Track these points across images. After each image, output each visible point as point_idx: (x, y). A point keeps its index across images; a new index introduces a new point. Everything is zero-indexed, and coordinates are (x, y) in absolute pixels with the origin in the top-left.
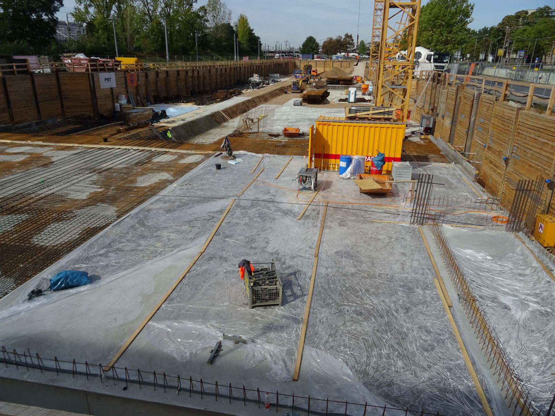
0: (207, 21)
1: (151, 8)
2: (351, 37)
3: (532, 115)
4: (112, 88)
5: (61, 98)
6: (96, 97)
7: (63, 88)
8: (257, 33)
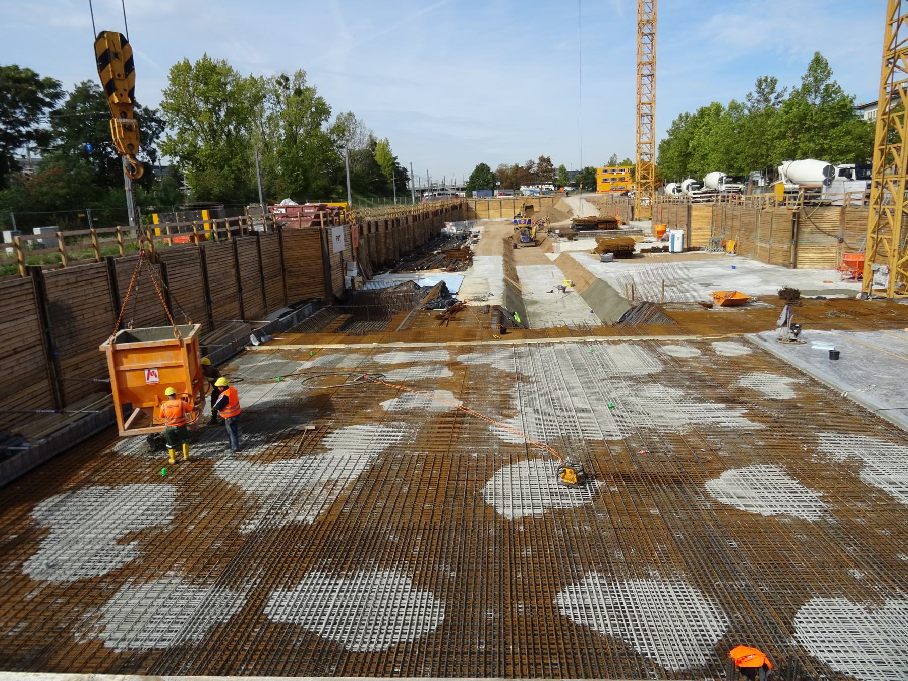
1: (268, 131)
2: (548, 160)
5: (284, 270)
8: (402, 163)
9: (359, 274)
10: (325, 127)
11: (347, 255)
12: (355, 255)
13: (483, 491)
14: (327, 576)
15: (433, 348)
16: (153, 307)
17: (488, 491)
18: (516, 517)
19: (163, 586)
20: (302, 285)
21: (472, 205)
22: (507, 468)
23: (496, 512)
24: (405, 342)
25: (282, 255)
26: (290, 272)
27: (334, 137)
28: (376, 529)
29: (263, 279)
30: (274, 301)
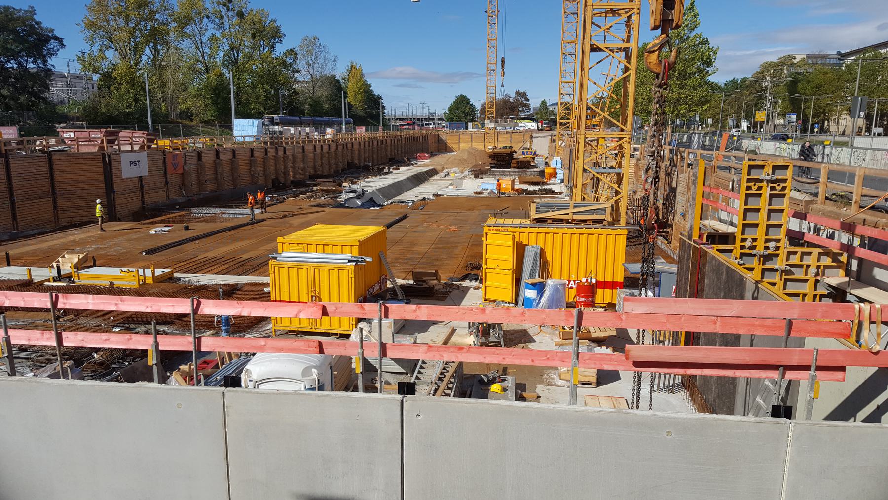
0: (298, 71)
2: (524, 95)
3: (830, 212)
4: (141, 177)
7: (58, 177)
10: (280, 49)
21: (444, 137)
27: (289, 60)
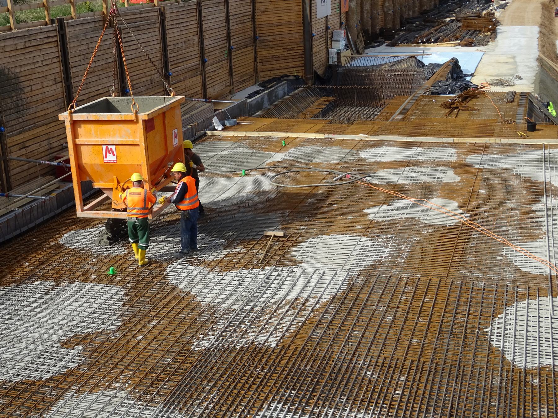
5: (255, 39)
6: (312, 36)
9: (347, 47)
11: (334, 22)
12: (344, 21)
13: (488, 330)
14: (289, 411)
15: (437, 145)
16: (105, 80)
17: (496, 331)
18: (530, 366)
19: (108, 398)
20: (277, 58)
22: (523, 305)
23: (503, 357)
24: (400, 134)
25: (254, 21)
26: (263, 41)
28: (351, 362)
29: (230, 49)
30: (241, 77)
